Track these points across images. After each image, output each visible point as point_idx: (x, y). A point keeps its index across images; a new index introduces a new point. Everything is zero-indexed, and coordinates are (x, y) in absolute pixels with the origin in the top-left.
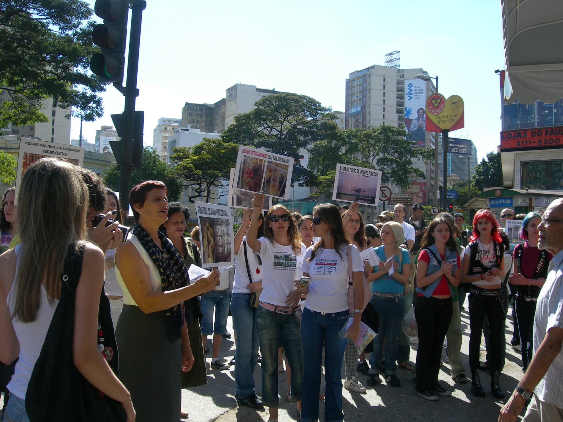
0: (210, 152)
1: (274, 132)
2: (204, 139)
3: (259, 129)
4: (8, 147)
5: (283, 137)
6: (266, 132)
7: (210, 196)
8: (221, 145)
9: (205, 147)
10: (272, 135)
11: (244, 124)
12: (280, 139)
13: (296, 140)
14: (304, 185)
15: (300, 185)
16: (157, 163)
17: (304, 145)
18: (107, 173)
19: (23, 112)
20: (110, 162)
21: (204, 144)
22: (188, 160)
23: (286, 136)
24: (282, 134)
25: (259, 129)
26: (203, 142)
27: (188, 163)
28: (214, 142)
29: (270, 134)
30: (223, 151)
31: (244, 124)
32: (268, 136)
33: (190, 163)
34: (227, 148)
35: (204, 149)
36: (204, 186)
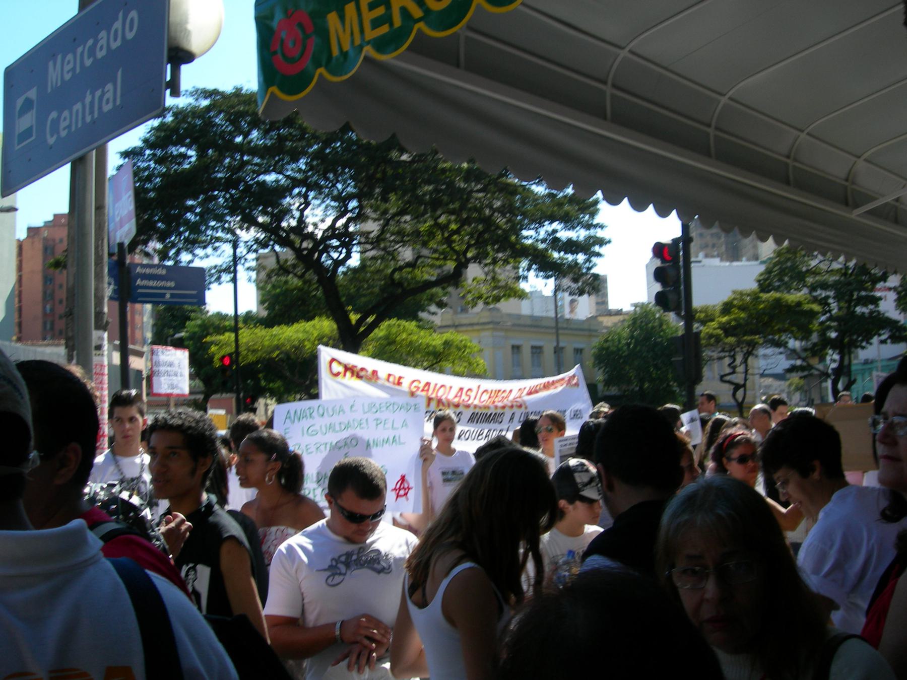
0: (742, 308)
1: (836, 266)
2: (734, 292)
3: (813, 263)
4: (457, 323)
5: (850, 271)
6: (824, 267)
7: (750, 371)
8: (758, 298)
9: (735, 302)
10: (832, 271)
11: (789, 259)
12: (845, 274)
13: (869, 273)
14: (889, 341)
15: (883, 342)
16: (664, 327)
17: (884, 278)
18: (596, 346)
19: (495, 288)
20: (596, 331)
21: (734, 299)
22: (714, 324)
23: (854, 269)
24: (847, 268)
25: (813, 263)
26: (733, 297)
27: (715, 329)
28: (748, 295)
29: (829, 270)
30: (762, 306)
31: (789, 259)
32: (827, 272)
33: (718, 328)
34: (768, 301)
35: (734, 306)
36: (739, 358)
